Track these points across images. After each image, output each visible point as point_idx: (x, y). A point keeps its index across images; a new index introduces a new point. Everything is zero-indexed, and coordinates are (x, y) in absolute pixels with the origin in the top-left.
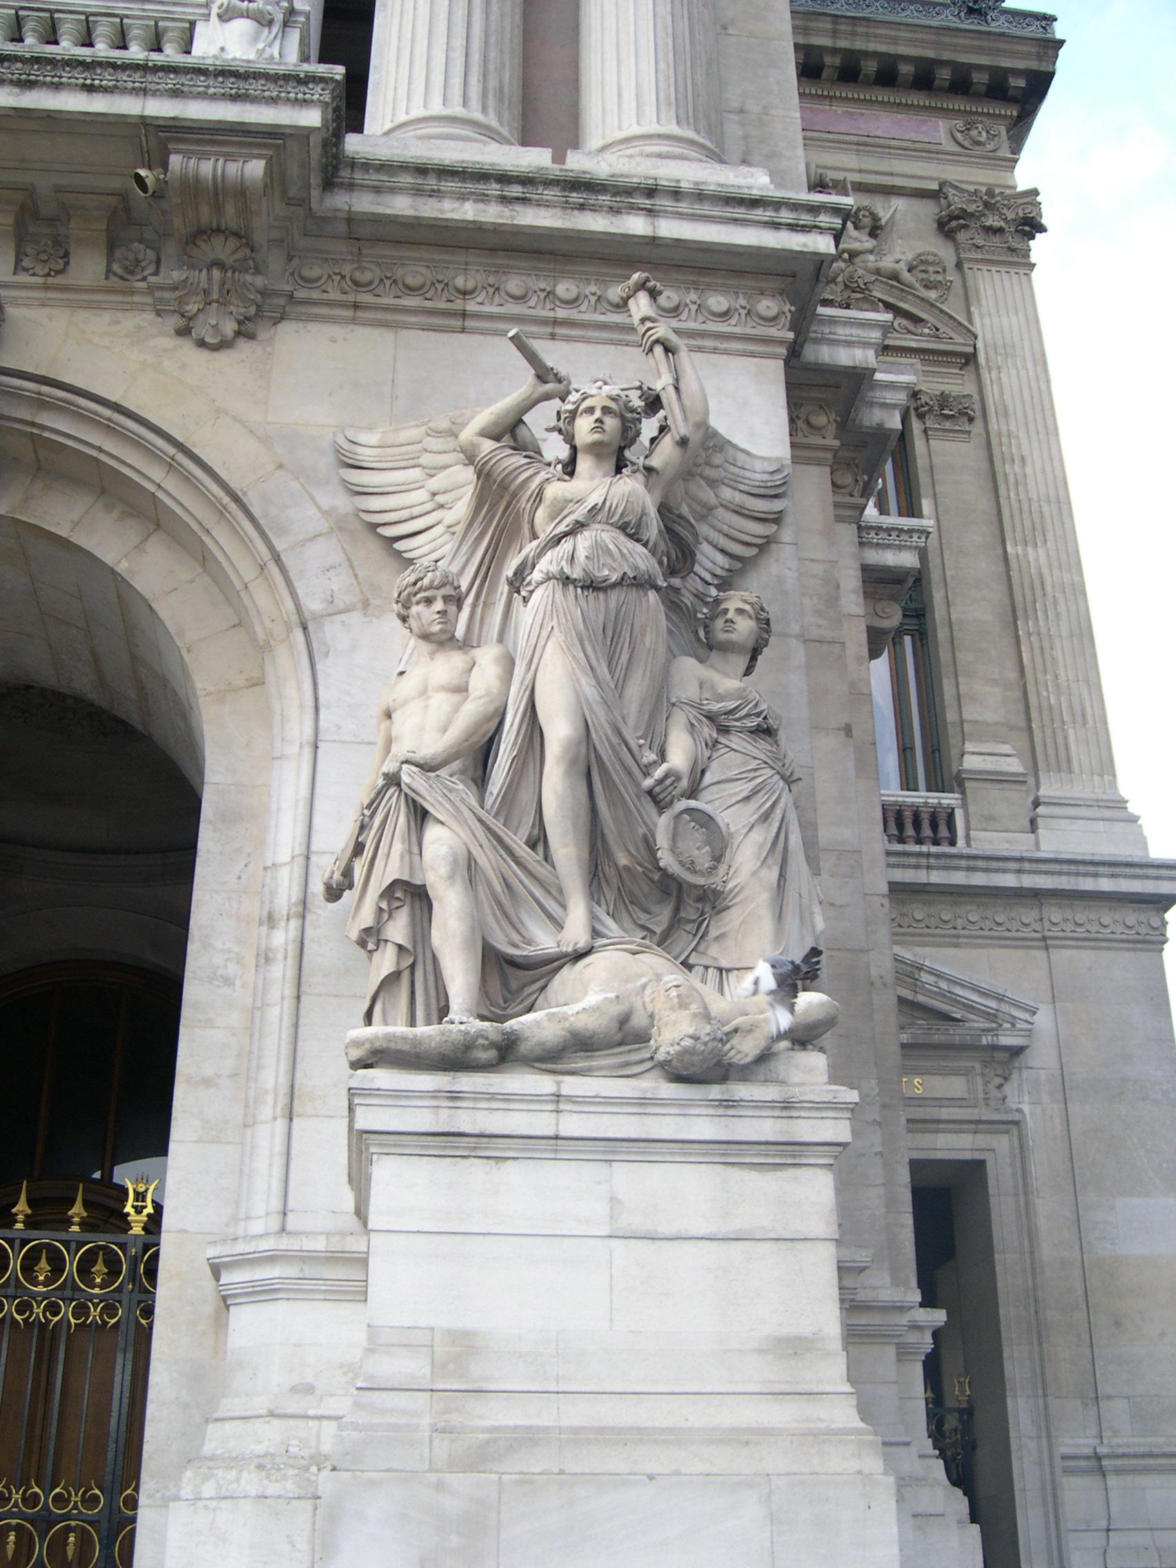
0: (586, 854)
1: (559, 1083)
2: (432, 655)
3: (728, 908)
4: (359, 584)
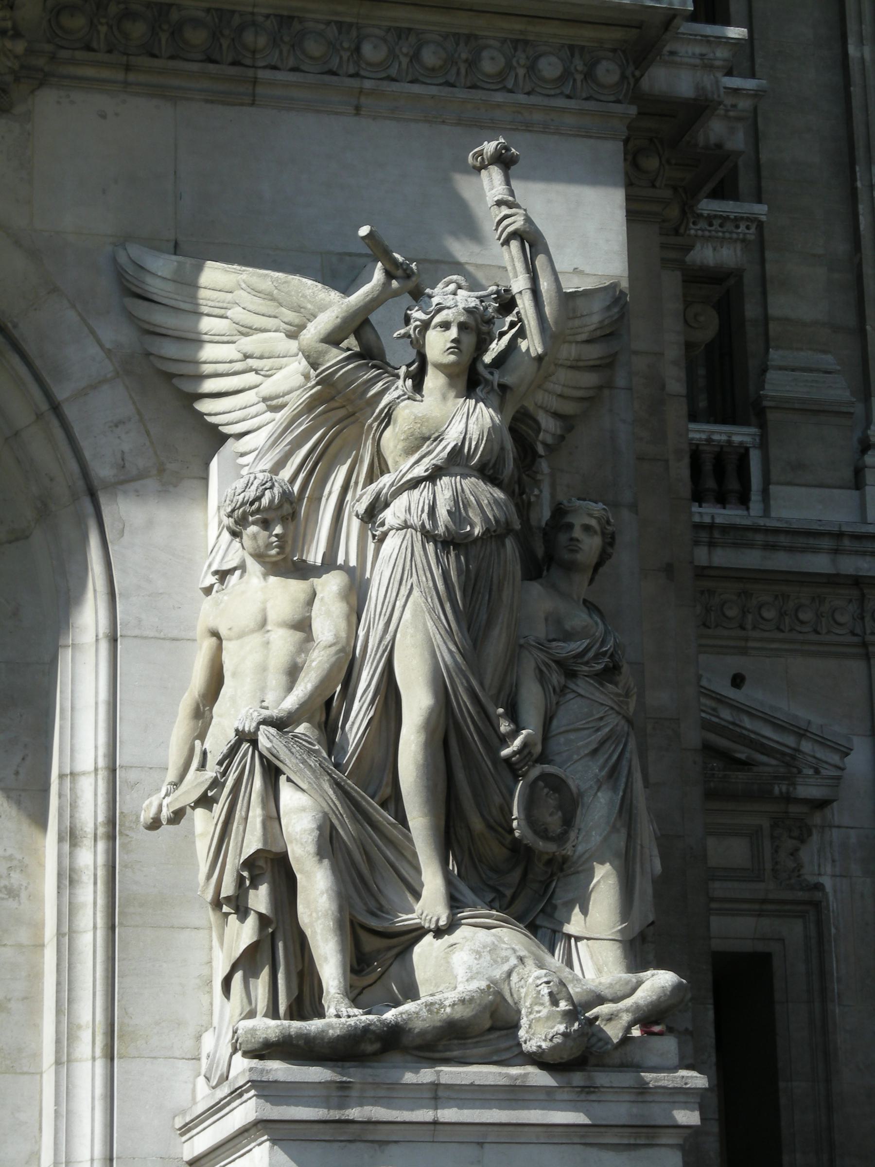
0: (443, 823)
1: (438, 1072)
2: (265, 575)
3: (578, 872)
4: (152, 443)
